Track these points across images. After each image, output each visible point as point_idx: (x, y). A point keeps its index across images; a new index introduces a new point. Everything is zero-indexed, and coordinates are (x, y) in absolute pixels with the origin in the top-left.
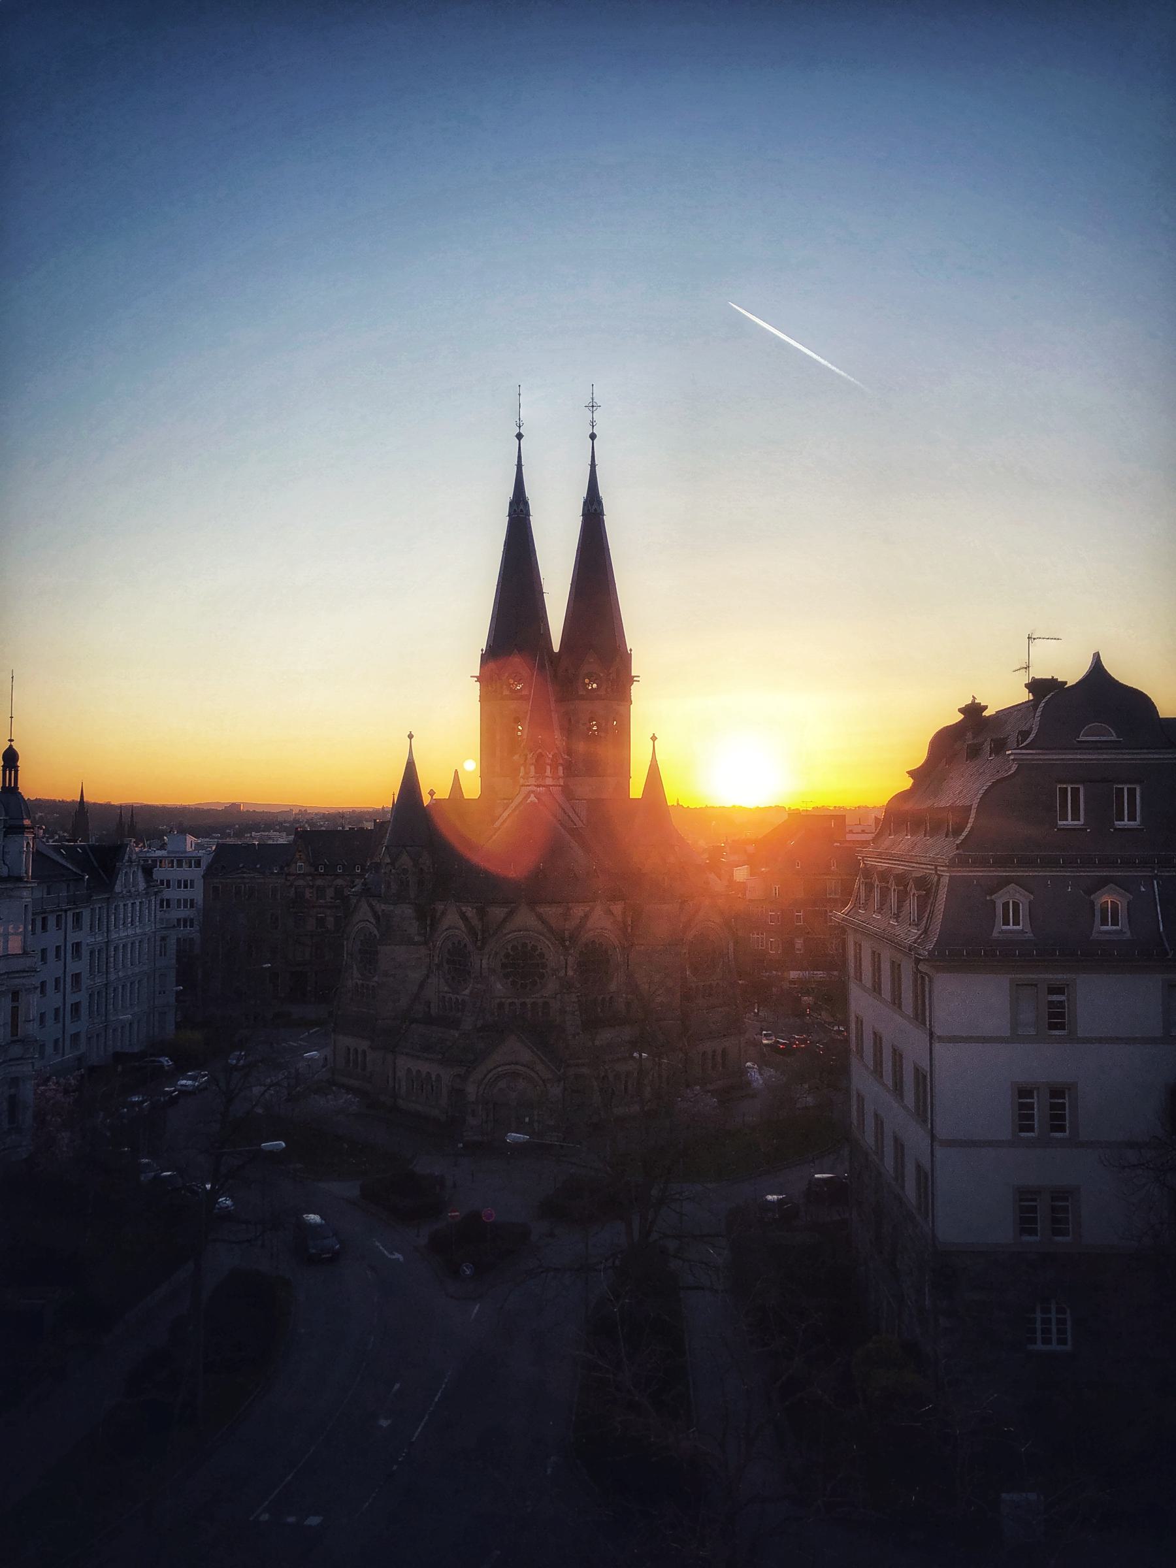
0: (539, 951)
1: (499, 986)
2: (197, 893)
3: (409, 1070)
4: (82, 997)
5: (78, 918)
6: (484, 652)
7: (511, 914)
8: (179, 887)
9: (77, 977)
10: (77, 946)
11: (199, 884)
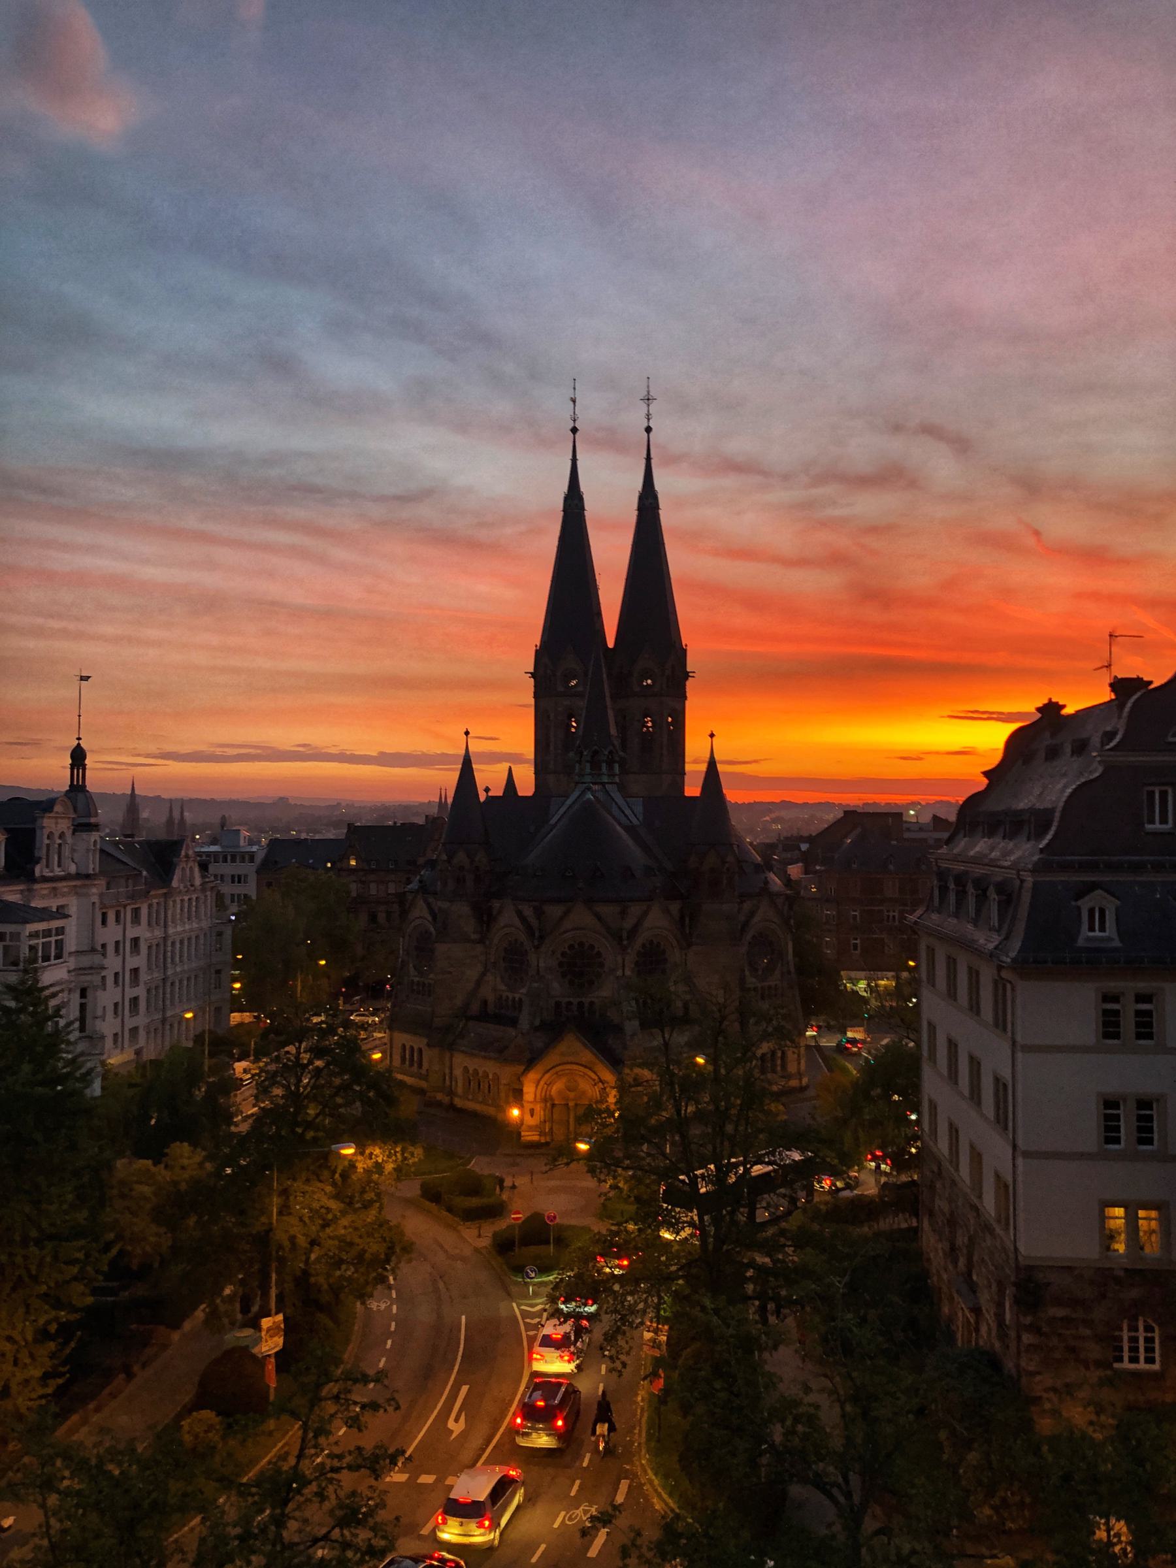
1: (556, 985)
2: (250, 889)
3: (466, 1069)
4: (140, 992)
5: (136, 913)
6: (538, 648)
7: (566, 913)
8: (233, 882)
9: (135, 971)
10: (136, 941)
11: (253, 879)
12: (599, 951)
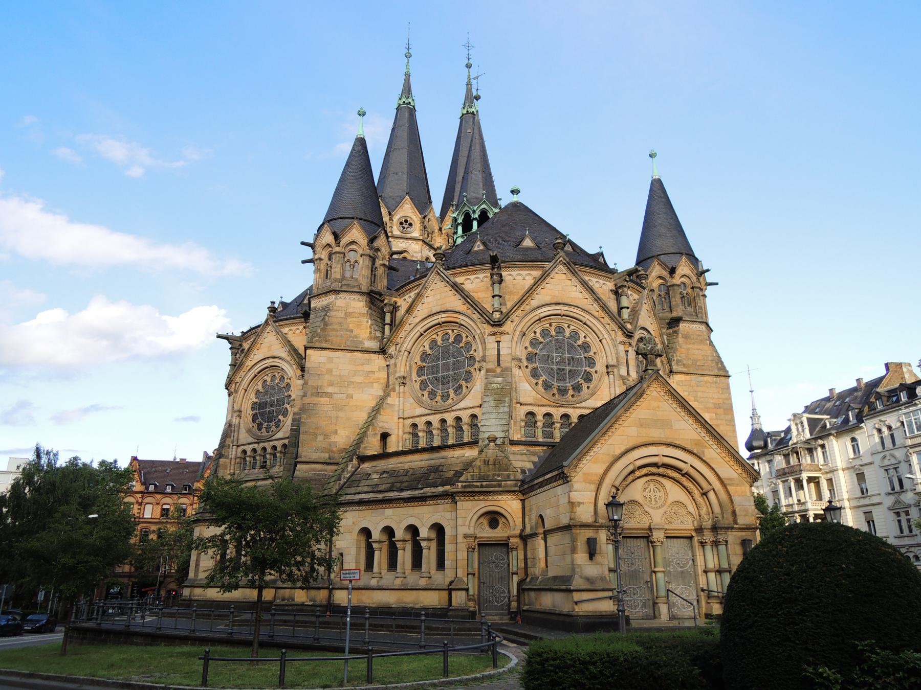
0: (582, 339)
1: (527, 387)
3: (366, 532)
12: (585, 343)
